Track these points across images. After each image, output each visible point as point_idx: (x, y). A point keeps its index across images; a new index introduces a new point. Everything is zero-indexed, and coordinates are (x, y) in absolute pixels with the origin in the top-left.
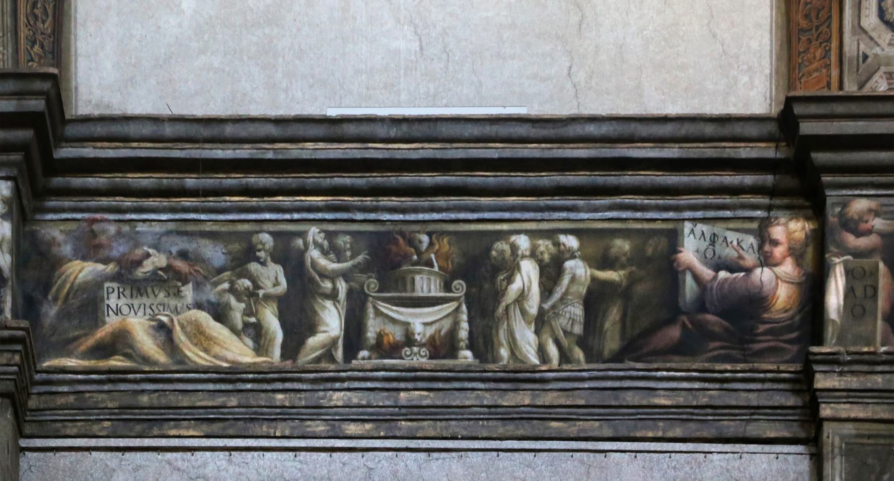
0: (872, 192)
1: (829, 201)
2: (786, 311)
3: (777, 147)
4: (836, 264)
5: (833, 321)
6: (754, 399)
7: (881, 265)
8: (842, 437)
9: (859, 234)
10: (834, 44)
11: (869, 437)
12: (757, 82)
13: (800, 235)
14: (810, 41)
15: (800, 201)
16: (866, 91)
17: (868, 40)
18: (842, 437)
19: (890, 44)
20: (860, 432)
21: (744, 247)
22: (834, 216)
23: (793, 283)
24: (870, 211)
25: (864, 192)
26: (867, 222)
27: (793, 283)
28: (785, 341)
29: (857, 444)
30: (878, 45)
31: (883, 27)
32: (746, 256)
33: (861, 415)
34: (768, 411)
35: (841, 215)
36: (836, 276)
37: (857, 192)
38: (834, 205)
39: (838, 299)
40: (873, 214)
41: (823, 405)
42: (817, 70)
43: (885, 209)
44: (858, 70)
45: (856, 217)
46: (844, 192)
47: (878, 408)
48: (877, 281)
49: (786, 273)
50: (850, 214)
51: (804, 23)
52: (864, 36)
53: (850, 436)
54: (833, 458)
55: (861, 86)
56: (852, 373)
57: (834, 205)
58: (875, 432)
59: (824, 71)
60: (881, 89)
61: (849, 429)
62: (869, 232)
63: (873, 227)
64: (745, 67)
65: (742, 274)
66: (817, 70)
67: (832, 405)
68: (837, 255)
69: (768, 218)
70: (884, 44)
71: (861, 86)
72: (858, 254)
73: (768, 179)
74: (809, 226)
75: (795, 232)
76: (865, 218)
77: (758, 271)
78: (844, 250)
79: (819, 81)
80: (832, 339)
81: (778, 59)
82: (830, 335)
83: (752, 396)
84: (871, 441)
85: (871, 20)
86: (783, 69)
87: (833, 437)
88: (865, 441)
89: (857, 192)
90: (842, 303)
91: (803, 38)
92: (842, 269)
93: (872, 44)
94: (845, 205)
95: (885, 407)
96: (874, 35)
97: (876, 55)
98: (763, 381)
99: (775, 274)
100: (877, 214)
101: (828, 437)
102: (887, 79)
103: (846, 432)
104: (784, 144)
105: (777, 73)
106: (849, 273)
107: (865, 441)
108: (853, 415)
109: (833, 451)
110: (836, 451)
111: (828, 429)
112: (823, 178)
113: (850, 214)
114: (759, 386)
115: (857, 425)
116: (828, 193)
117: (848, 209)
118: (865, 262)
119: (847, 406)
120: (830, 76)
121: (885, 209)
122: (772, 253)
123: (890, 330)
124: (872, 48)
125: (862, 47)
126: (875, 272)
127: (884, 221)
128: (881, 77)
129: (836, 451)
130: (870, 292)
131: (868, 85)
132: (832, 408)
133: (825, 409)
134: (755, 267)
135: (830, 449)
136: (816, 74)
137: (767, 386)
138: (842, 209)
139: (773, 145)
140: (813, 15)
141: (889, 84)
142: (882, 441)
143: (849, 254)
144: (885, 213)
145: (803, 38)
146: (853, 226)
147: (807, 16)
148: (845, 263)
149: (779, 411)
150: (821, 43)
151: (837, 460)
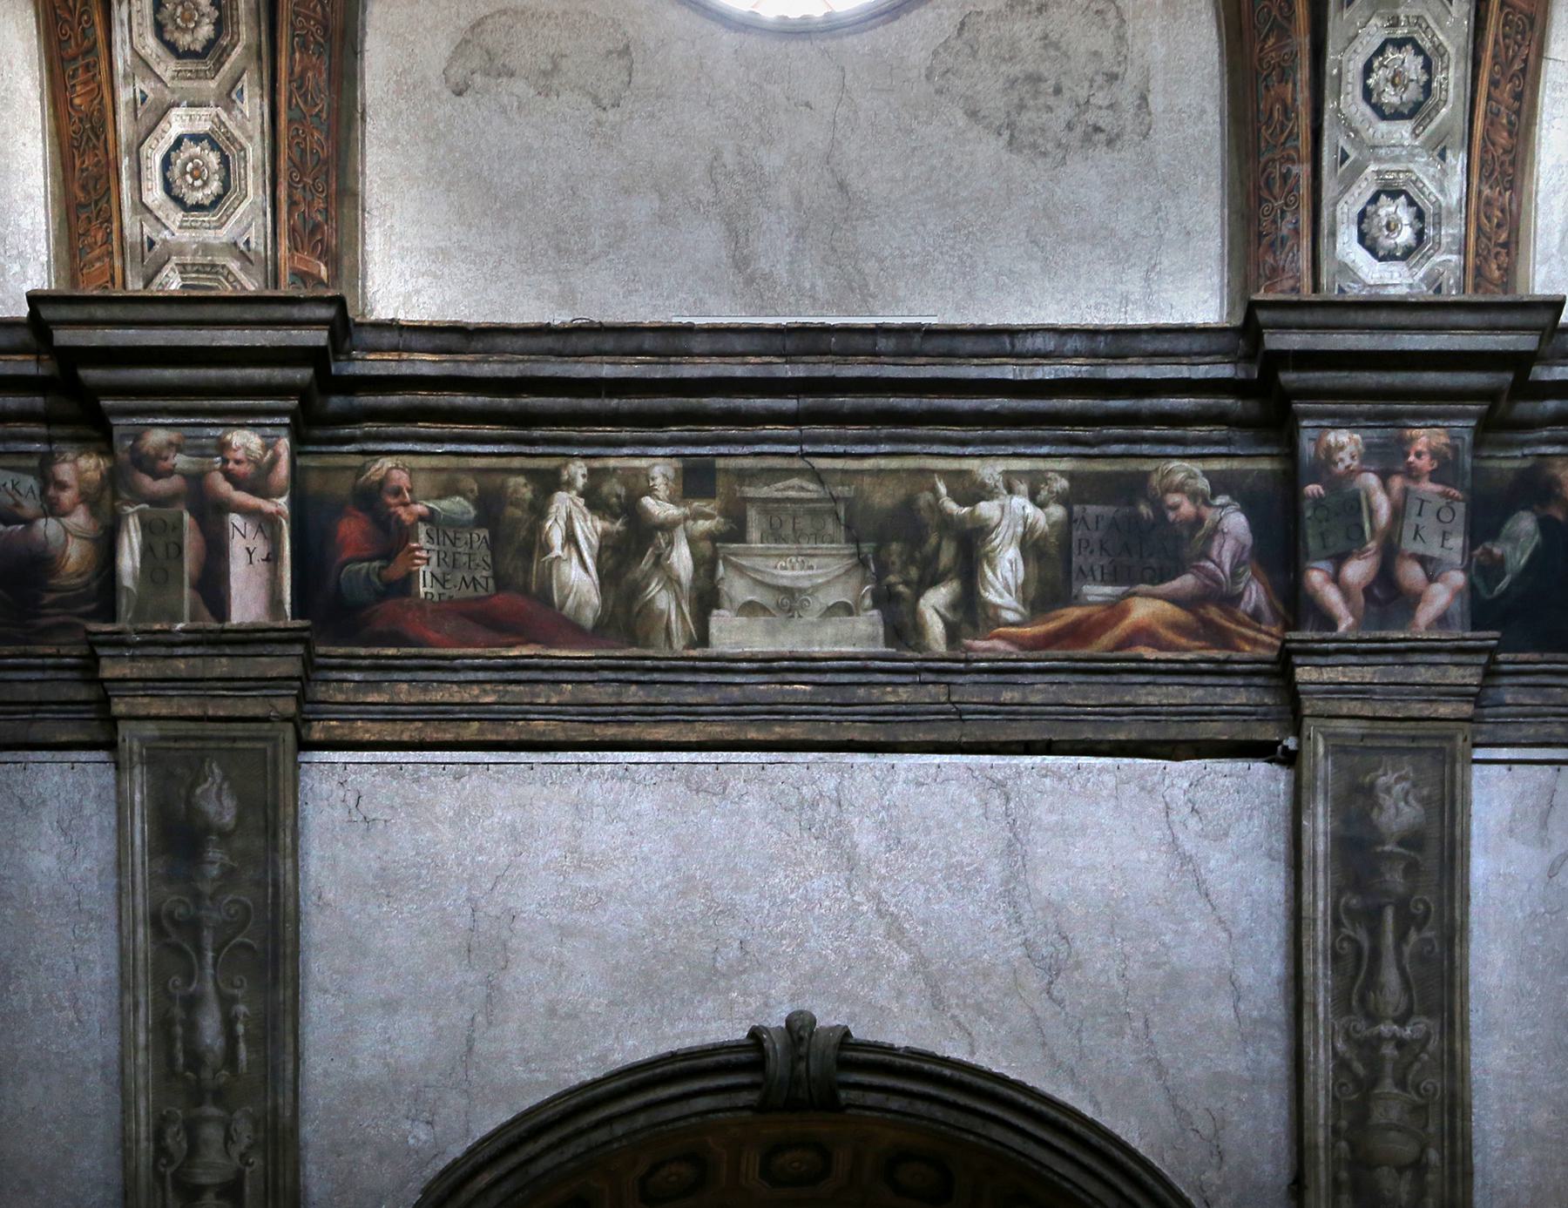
0: (170, 421)
1: (116, 432)
2: (80, 576)
3: (38, 360)
4: (128, 515)
5: (128, 589)
6: (33, 693)
7: (187, 517)
8: (142, 740)
9: (157, 475)
10: (115, 225)
11: (176, 739)
12: (30, 273)
13: (94, 476)
14: (89, 220)
15: (83, 431)
16: (154, 290)
17: (153, 221)
18: (142, 740)
19: (180, 227)
20: (164, 733)
21: (22, 491)
22: (124, 452)
23: (86, 538)
24: (170, 444)
25: (160, 421)
26: (166, 459)
27: (86, 538)
28: (80, 616)
29: (162, 748)
30: (167, 228)
31: (171, 204)
32: (25, 503)
33: (164, 712)
34: (54, 707)
35: (133, 449)
36: (129, 532)
37: (150, 421)
38: (124, 436)
39: (133, 559)
40: (174, 449)
41: (116, 700)
42: (98, 259)
43: (189, 442)
44: (143, 261)
45: (152, 452)
46: (135, 420)
47: (184, 702)
48: (181, 537)
49: (77, 525)
50: (145, 449)
51: (81, 196)
52: (148, 215)
53: (154, 739)
54: (132, 768)
55: (148, 282)
56: (148, 657)
57: (124, 436)
58: (183, 733)
59: (107, 260)
60: (173, 287)
61: (150, 729)
62: (170, 473)
63: (174, 465)
64: (15, 252)
65: (20, 527)
66: (98, 259)
67: (127, 699)
68: (129, 503)
69: (51, 453)
70: (174, 228)
71: (148, 282)
72: (156, 501)
73: (38, 402)
74: (104, 463)
75: (87, 471)
76: (165, 454)
77: (42, 522)
78: (138, 496)
79: (103, 273)
80: (127, 611)
81: (58, 241)
82: (124, 608)
83: (33, 688)
84: (177, 745)
85: (155, 194)
86: (65, 256)
87: (131, 741)
88: (172, 744)
89: (150, 421)
90: (138, 565)
91: (83, 217)
92: (137, 521)
93: (159, 226)
94: (137, 438)
95: (194, 700)
96: (160, 214)
97: (165, 241)
98: (43, 668)
99: (64, 527)
100: (179, 448)
101: (124, 740)
102: (181, 273)
103: (148, 733)
104: (46, 357)
105: (56, 260)
106: (147, 527)
107: (172, 744)
108: (153, 712)
109: (131, 759)
110: (136, 758)
111: (124, 729)
112: (102, 403)
113: (145, 449)
114: (38, 675)
115: (163, 724)
116: (114, 421)
117: (142, 442)
118: (167, 513)
119: (146, 700)
120: (112, 267)
121: (189, 442)
122: (58, 499)
123: (200, 600)
124: (159, 232)
125: (146, 229)
126: (178, 526)
127: (188, 458)
128: (172, 269)
129: (136, 758)
130: (173, 550)
131: (157, 281)
132: (126, 704)
133: (117, 704)
134: (37, 517)
135: (127, 756)
136: (98, 265)
137: (49, 674)
138: (135, 441)
139: (32, 357)
140: (91, 186)
141: (183, 279)
142: (193, 744)
143: (146, 502)
144: (190, 447)
145: (83, 217)
146: (150, 464)
147: (84, 187)
148: (141, 514)
149: (70, 707)
150: (102, 223)
151: (137, 771)
